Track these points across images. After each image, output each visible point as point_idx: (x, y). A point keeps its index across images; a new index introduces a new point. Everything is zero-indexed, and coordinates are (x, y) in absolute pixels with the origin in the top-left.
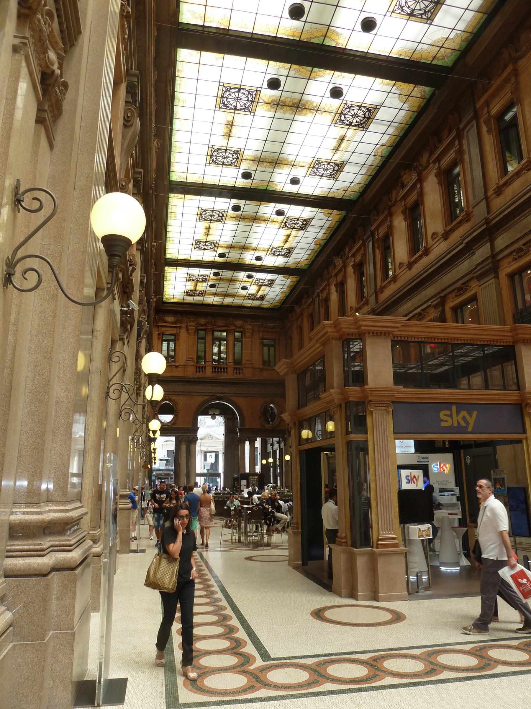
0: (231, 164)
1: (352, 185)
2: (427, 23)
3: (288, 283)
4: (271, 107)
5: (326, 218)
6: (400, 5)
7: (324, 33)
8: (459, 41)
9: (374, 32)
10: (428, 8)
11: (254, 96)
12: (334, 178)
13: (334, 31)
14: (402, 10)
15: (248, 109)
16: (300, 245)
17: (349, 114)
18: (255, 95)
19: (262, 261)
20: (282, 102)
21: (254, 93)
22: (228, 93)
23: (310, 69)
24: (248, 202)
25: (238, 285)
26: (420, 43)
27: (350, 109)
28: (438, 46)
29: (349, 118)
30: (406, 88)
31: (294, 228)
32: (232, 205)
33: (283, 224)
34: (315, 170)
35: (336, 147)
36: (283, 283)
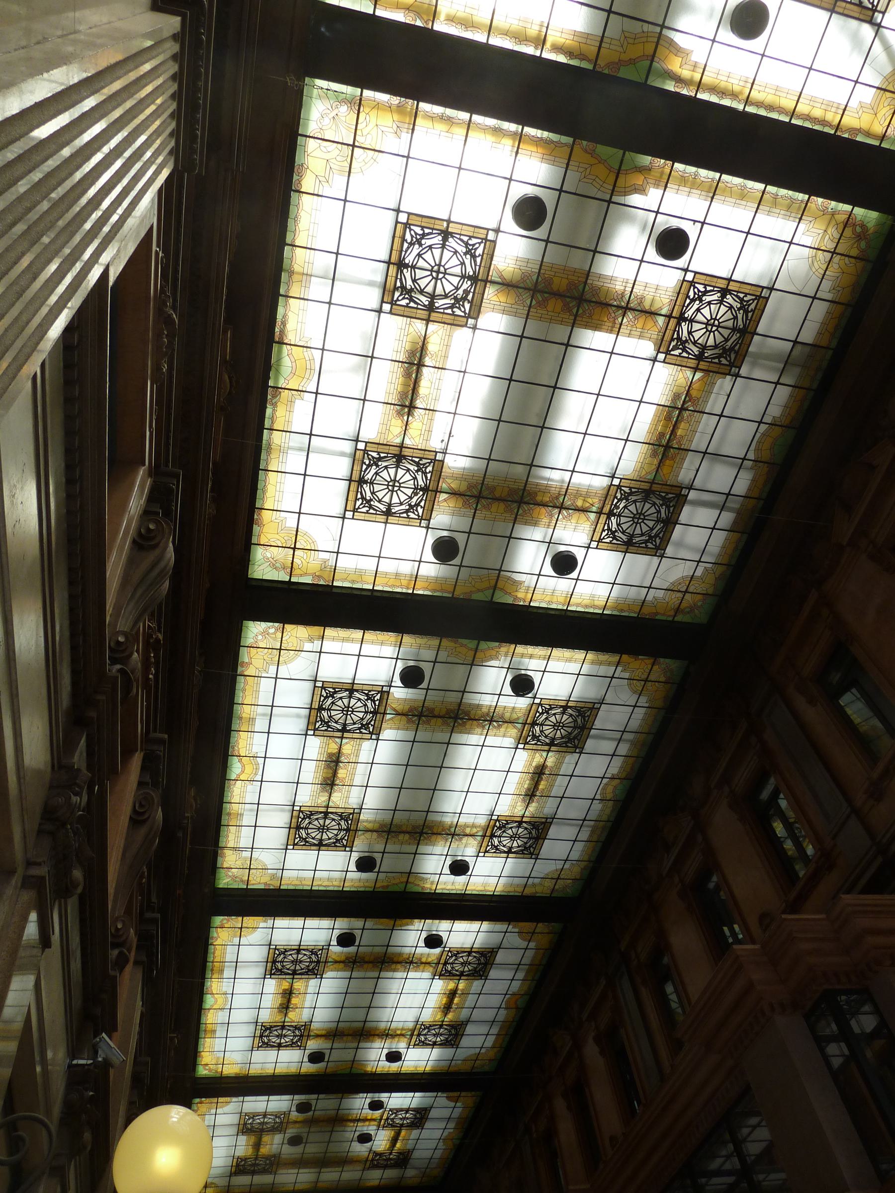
0: (336, 845)
2: (655, 555)
3: (457, 1112)
4: (409, 721)
5: (524, 944)
6: (609, 529)
7: (493, 583)
8: (711, 579)
9: (574, 575)
10: (654, 532)
11: (377, 703)
12: (532, 854)
13: (509, 578)
14: (614, 538)
16: (477, 1014)
17: (548, 723)
18: (380, 700)
19: (399, 1064)
20: (428, 709)
21: (378, 697)
22: (330, 700)
23: (472, 644)
24: (370, 923)
25: (351, 1132)
26: (650, 587)
27: (548, 713)
28: (679, 591)
29: (548, 730)
30: (640, 665)
31: (462, 974)
32: (336, 933)
33: (440, 966)
34: (496, 841)
35: (529, 789)
36: (446, 1113)
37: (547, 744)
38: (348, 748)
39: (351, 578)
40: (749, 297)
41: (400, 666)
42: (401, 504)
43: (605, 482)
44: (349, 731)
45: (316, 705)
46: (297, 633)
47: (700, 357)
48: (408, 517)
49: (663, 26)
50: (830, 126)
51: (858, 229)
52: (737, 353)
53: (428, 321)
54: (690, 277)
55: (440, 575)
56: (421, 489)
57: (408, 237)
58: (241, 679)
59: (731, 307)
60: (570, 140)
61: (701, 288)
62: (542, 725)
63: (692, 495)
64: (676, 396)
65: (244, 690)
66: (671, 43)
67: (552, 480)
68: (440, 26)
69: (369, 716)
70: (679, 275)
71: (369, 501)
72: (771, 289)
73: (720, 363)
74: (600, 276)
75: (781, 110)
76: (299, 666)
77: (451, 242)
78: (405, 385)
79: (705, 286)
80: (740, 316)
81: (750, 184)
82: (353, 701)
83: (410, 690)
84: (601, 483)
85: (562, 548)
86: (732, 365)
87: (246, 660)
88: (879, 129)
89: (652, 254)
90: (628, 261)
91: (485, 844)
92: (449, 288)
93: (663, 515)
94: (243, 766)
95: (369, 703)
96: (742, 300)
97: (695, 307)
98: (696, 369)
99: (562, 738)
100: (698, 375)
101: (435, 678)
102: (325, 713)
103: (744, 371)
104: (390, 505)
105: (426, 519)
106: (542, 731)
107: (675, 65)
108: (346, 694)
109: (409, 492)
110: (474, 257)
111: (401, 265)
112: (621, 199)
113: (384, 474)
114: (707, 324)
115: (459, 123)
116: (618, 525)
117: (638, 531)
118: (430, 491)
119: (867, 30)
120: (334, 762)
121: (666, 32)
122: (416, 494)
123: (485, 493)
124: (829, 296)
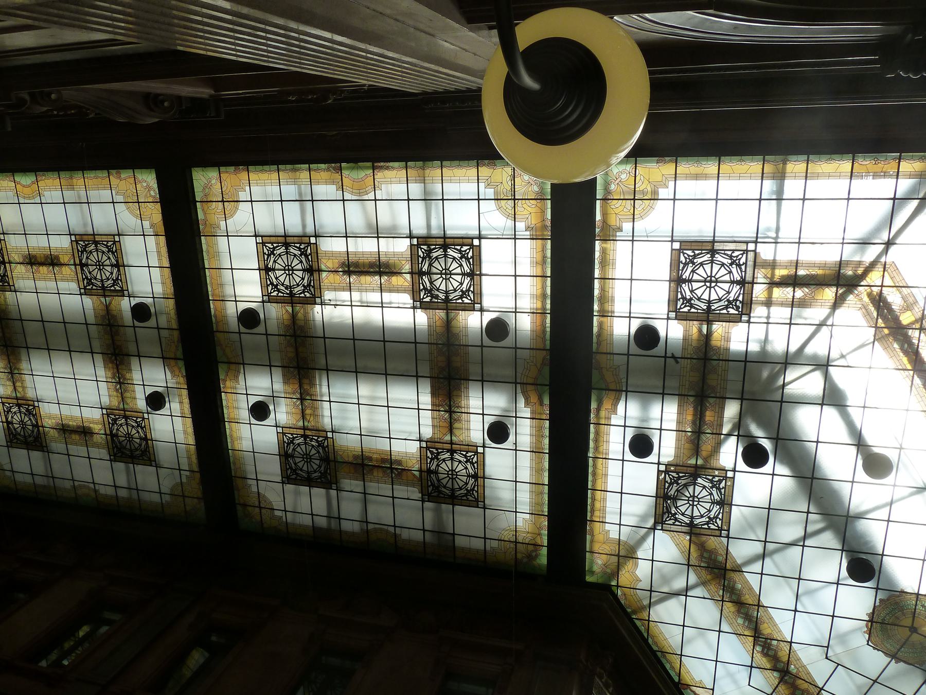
1: (8, 474)
4: (103, 317)
6: (294, 438)
7: (233, 360)
12: (11, 441)
13: (239, 372)
14: (288, 444)
15: (88, 284)
17: (130, 428)
18: (115, 291)
21: (118, 288)
22: (105, 250)
23: (180, 354)
26: (257, 480)
30: (195, 488)
34: (15, 409)
35: (69, 426)
37: (111, 432)
38: (67, 271)
39: (211, 250)
40: (476, 494)
41: (149, 301)
42: (276, 278)
43: (329, 428)
44: (82, 270)
45: (98, 238)
46: (155, 213)
47: (429, 471)
48: (268, 285)
49: (627, 391)
50: (592, 516)
51: (534, 554)
52: (438, 496)
53: (412, 273)
54: (480, 450)
55: (229, 319)
56: (291, 291)
57: (465, 248)
58: (105, 173)
59: (467, 484)
60: (548, 347)
61: (475, 460)
62: (127, 424)
63: (333, 493)
64: (399, 462)
65: (96, 178)
66: (617, 400)
67: (321, 388)
68: (598, 245)
69: (99, 284)
70: (480, 442)
71: (273, 253)
72: (484, 508)
73: (428, 486)
74: (467, 388)
75: (594, 482)
76: (128, 219)
77: (467, 280)
78: (364, 265)
79: (477, 462)
80: (462, 491)
81: (546, 474)
82: (109, 268)
83: (130, 313)
84: (326, 422)
85: (271, 407)
86: (429, 495)
87: (123, 176)
88: (596, 548)
89: (489, 420)
90: (482, 405)
91: (9, 401)
92: (437, 283)
93: (314, 475)
94: (29, 186)
95: (110, 282)
96: (473, 490)
97: (462, 459)
98: (420, 471)
99: (120, 443)
100: (417, 473)
101: (145, 331)
102: (93, 247)
103: (427, 504)
104: (274, 270)
105: (268, 299)
106: (121, 425)
107: (607, 405)
108: (114, 262)
109: (287, 283)
110: (461, 297)
111: (445, 247)
112: (519, 390)
113: (296, 262)
114: (452, 470)
115: (543, 270)
116: (299, 444)
117: (298, 460)
118: (291, 299)
119: (650, 523)
120: (52, 261)
121: (624, 394)
122: (286, 288)
123: (299, 340)
124: (488, 548)
